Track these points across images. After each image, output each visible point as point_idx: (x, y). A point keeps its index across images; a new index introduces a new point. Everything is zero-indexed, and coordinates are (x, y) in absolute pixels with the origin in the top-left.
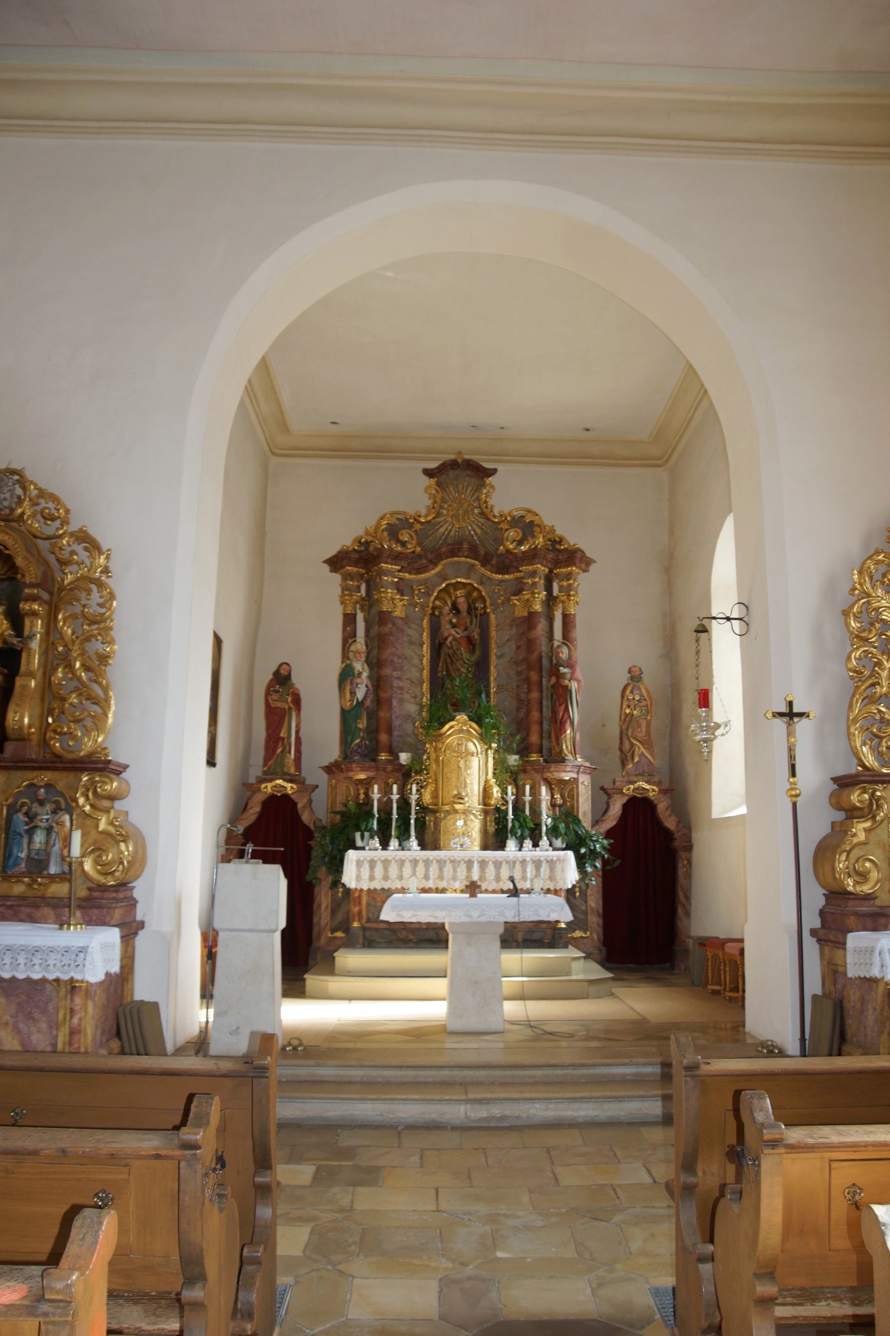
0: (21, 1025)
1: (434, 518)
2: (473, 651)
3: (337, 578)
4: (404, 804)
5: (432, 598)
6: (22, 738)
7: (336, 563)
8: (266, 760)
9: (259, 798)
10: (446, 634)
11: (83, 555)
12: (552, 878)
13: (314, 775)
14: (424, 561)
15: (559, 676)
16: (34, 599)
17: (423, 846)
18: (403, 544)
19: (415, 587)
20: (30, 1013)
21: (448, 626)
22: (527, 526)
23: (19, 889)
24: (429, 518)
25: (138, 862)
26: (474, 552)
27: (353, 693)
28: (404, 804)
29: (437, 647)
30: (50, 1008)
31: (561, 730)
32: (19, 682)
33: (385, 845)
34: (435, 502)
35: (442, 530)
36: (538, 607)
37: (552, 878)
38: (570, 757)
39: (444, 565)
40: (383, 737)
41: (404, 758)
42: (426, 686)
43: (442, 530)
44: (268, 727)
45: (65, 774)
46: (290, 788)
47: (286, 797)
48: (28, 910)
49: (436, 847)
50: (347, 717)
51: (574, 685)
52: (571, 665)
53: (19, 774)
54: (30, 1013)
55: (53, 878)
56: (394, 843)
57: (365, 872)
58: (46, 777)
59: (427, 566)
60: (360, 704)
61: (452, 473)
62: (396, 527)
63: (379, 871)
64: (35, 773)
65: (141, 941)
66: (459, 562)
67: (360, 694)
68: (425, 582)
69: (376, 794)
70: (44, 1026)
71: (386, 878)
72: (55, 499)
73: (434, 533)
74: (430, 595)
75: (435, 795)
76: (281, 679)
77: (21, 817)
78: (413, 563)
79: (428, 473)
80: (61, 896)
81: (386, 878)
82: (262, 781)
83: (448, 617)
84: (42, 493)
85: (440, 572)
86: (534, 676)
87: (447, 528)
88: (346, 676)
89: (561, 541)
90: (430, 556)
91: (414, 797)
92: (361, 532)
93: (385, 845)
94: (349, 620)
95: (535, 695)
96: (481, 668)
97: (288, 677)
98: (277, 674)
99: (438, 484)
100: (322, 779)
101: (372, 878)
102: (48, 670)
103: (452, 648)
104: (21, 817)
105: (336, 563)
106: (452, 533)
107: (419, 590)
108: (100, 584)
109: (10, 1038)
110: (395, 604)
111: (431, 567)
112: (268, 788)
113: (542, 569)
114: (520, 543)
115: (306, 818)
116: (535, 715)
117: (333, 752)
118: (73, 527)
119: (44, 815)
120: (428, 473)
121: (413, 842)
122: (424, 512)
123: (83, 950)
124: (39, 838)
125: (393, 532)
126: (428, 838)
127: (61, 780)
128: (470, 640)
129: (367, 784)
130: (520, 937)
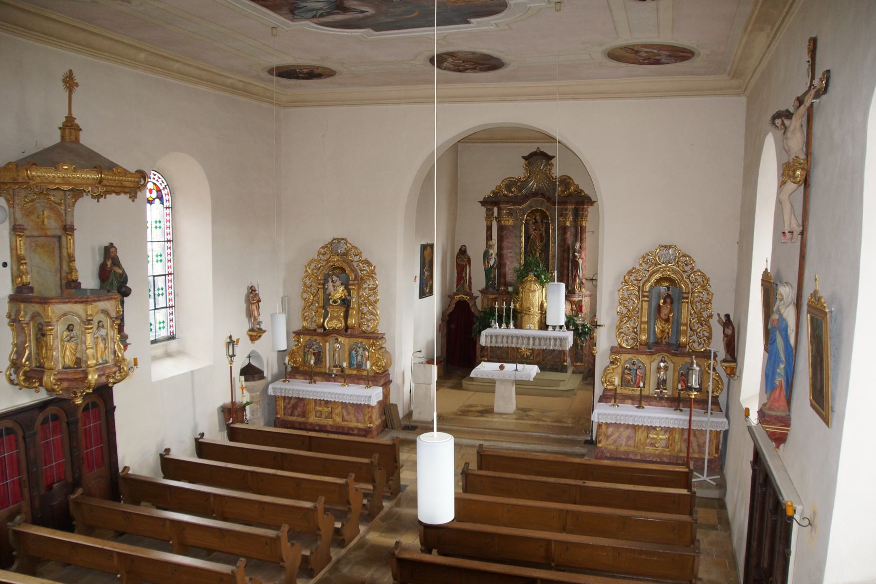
2: (542, 241)
3: (484, 209)
4: (508, 309)
6: (353, 328)
7: (484, 203)
8: (457, 286)
9: (454, 301)
11: (367, 268)
12: (561, 346)
13: (475, 291)
15: (575, 257)
16: (353, 285)
17: (516, 326)
18: (513, 192)
22: (566, 181)
23: (355, 372)
25: (389, 363)
26: (543, 195)
27: (488, 263)
28: (508, 309)
29: (527, 238)
31: (574, 280)
33: (500, 326)
36: (568, 224)
37: (561, 346)
38: (577, 291)
40: (502, 280)
41: (510, 289)
42: (523, 256)
44: (458, 273)
46: (466, 298)
47: (465, 301)
49: (521, 328)
50: (488, 272)
51: (581, 261)
52: (580, 252)
56: (504, 325)
57: (489, 339)
58: (360, 340)
60: (492, 267)
61: (535, 157)
62: (510, 184)
63: (494, 339)
65: (391, 386)
67: (492, 262)
68: (520, 210)
69: (497, 306)
71: (496, 342)
72: (356, 248)
75: (521, 306)
76: (463, 252)
77: (354, 352)
78: (516, 201)
79: (525, 158)
82: (455, 294)
83: (532, 228)
84: (353, 247)
86: (566, 255)
87: (533, 184)
88: (486, 256)
89: (582, 191)
91: (512, 306)
92: (494, 189)
93: (500, 326)
94: (489, 228)
95: (566, 263)
96: (546, 249)
97: (465, 251)
98: (460, 250)
100: (480, 295)
101: (491, 342)
102: (359, 306)
104: (354, 352)
105: (484, 203)
108: (372, 277)
110: (509, 222)
112: (457, 297)
113: (571, 207)
114: (564, 192)
115: (473, 310)
116: (566, 272)
117: (483, 285)
118: (363, 259)
119: (361, 351)
120: (525, 158)
121: (512, 326)
124: (359, 358)
125: (508, 187)
126: (518, 322)
127: (365, 341)
128: (541, 235)
129: (495, 300)
130: (548, 367)
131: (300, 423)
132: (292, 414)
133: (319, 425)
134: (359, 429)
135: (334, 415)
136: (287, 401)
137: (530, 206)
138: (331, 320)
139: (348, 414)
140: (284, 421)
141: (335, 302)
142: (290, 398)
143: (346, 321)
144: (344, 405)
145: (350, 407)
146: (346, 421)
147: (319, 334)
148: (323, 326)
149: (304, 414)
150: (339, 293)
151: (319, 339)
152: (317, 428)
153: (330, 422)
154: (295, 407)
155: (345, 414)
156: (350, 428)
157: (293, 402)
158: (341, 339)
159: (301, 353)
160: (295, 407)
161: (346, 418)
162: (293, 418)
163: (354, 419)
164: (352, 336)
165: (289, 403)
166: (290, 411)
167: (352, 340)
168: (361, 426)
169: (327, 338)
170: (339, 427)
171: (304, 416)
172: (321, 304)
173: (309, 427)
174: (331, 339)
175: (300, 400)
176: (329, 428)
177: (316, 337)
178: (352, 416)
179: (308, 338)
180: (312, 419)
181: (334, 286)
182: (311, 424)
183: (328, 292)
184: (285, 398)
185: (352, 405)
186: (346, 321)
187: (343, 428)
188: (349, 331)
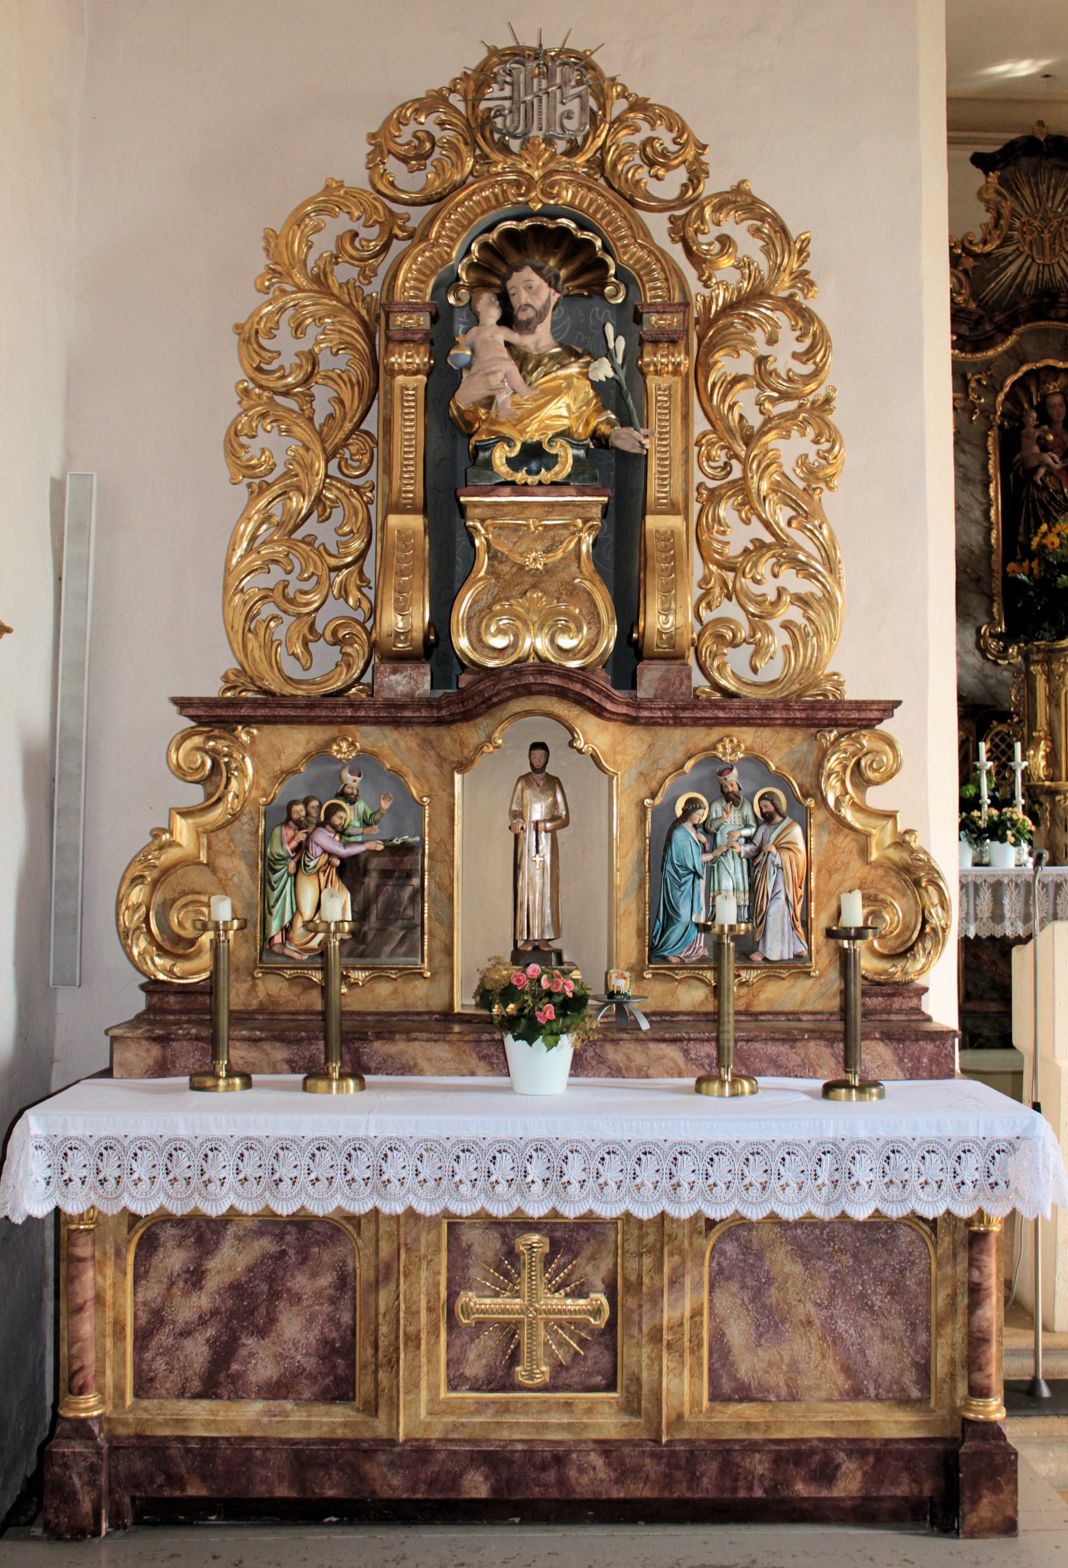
0: (841, 1325)
1: (997, 248)
5: (1001, 397)
10: (1034, 463)
14: (988, 328)
19: (969, 375)
20: (863, 1295)
21: (1036, 449)
23: (692, 996)
24: (989, 248)
30: (911, 1283)
32: (653, 523)
34: (999, 215)
35: (1012, 269)
39: (1021, 335)
43: (1012, 269)
45: (785, 733)
48: (772, 1049)
53: (678, 734)
54: (863, 1295)
55: (773, 969)
59: (992, 337)
64: (716, 733)
66: (1046, 331)
68: (988, 364)
70: (897, 1324)
73: (998, 274)
74: (997, 393)
80: (787, 1008)
81: (997, 916)
85: (1012, 348)
90: (998, 318)
99: (1002, 181)
103: (1045, 487)
106: (1032, 277)
107: (979, 381)
109: (816, 1356)
111: (999, 337)
119: (733, 823)
122: (978, 236)
123: (1009, 1148)
131: (304, 1457)
132: (217, 1381)
133: (493, 1459)
134: (878, 1454)
135: (634, 1355)
136: (174, 1258)
137: (1018, 357)
138: (514, 581)
139: (770, 1322)
140: (152, 1448)
141: (534, 455)
142: (203, 1232)
143: (628, 610)
144: (739, 1247)
145: (783, 1263)
146: (744, 1394)
147: (394, 714)
148: (435, 649)
149: (338, 1370)
150: (562, 408)
151: (394, 746)
152: (477, 1485)
153: (604, 1418)
154: (248, 1309)
155: (737, 1333)
156: (793, 1455)
157: (229, 1261)
158: (595, 734)
159: (239, 869)
160: (248, 1309)
161: (749, 1364)
162: (242, 1416)
163: (822, 1372)
164: (683, 711)
165: (195, 1277)
166: (197, 1352)
167: (677, 741)
168: (894, 1424)
169: (472, 734)
170: (684, 1459)
171: (340, 1390)
172: (410, 482)
173: (390, 1482)
174: (504, 740)
175: (304, 1235)
176: (593, 1477)
177: (368, 737)
178: (803, 1349)
179: (295, 742)
180: (428, 1404)
181: (520, 357)
182: (421, 1451)
183: (466, 396)
184: (149, 1234)
185: (812, 1238)
186: (628, 610)
187: (726, 1453)
188: (650, 678)
